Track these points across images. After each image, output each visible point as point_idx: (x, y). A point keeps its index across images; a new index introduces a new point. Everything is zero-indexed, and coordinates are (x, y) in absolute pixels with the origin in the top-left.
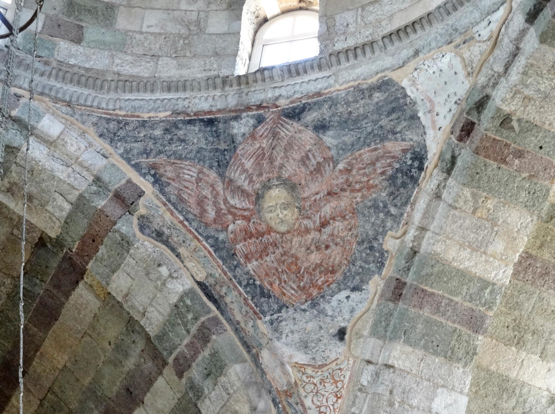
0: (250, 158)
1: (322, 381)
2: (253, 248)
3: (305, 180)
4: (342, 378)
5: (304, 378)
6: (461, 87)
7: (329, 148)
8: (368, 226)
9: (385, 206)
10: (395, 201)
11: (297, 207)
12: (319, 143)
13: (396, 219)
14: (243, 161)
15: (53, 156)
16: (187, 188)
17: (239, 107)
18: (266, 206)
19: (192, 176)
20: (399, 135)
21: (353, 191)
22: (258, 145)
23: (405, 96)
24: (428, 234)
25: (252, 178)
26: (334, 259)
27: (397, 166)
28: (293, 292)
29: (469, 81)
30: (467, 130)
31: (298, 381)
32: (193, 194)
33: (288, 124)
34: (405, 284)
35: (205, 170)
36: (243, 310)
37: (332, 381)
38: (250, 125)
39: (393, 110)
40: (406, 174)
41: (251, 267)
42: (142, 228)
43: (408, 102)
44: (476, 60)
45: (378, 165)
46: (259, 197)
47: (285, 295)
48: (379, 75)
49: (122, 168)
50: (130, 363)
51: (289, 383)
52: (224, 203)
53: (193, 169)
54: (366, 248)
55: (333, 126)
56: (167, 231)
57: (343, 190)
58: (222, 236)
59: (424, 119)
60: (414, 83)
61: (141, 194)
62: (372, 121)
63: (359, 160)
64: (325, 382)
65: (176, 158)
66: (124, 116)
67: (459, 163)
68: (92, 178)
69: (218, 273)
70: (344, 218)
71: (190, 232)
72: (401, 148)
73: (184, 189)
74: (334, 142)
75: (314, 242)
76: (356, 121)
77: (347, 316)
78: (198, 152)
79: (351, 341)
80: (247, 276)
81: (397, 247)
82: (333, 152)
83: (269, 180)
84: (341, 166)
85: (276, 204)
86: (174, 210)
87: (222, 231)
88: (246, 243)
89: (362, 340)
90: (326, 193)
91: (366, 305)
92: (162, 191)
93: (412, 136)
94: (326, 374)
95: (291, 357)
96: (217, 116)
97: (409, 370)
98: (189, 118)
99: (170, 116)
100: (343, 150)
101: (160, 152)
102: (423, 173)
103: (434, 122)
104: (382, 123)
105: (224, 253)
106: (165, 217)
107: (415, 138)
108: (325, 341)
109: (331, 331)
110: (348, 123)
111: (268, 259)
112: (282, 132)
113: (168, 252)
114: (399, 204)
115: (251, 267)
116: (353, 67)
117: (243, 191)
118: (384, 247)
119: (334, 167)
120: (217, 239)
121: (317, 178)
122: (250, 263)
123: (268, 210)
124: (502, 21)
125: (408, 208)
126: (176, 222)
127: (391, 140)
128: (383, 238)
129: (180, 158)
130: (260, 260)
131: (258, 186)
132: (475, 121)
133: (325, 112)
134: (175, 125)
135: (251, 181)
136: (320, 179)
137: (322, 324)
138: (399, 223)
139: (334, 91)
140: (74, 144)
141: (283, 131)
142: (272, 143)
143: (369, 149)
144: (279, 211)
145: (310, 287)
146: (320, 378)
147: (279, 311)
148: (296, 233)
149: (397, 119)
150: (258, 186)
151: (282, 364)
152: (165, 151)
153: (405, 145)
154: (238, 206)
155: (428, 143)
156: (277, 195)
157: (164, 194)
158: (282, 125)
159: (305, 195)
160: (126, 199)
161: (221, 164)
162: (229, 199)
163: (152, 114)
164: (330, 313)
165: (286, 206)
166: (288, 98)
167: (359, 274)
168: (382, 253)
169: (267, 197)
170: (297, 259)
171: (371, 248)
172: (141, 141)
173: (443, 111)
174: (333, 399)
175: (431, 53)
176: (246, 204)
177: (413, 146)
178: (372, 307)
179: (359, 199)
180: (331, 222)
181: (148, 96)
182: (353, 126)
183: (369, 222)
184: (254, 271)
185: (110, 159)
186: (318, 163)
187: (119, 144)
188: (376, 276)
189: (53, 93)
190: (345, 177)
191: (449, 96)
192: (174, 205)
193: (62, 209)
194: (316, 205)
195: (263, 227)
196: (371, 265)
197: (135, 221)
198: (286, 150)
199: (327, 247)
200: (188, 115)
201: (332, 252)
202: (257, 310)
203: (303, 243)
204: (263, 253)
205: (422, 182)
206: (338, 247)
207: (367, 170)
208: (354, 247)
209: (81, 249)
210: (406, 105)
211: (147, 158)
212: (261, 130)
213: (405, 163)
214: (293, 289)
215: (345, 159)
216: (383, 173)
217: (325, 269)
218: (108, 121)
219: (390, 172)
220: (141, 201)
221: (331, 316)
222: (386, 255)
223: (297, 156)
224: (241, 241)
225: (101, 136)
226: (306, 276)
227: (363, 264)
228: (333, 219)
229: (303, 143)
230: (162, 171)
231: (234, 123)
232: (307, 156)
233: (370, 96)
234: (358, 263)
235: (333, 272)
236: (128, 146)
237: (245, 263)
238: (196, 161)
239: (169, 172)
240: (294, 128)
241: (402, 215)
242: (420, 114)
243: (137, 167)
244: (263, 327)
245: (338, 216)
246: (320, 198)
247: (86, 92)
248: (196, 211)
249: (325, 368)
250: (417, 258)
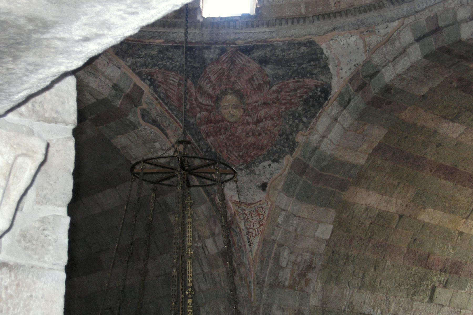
1: (251, 213)
3: (250, 93)
4: (263, 213)
5: (240, 210)
7: (268, 76)
8: (287, 126)
9: (300, 116)
10: (306, 114)
11: (243, 109)
13: (306, 125)
14: (210, 75)
15: (88, 71)
16: (172, 89)
17: (210, 42)
18: (222, 105)
20: (314, 76)
21: (281, 104)
22: (221, 67)
23: (322, 53)
24: (326, 140)
25: (215, 87)
27: (311, 94)
28: (235, 158)
29: (366, 55)
31: (235, 212)
32: (175, 93)
33: (242, 56)
34: (308, 165)
37: (257, 214)
38: (217, 53)
39: (312, 60)
40: (316, 99)
41: (209, 141)
42: (143, 117)
43: (323, 58)
44: (374, 44)
45: (299, 91)
46: (218, 99)
47: (229, 159)
48: (307, 37)
49: (130, 75)
52: (195, 101)
53: (176, 77)
54: (284, 138)
55: (271, 62)
57: (273, 102)
58: (192, 121)
60: (329, 47)
61: (142, 92)
62: (298, 63)
63: (286, 86)
64: (252, 214)
65: (165, 70)
66: (133, 41)
67: (352, 103)
68: (112, 84)
70: (272, 119)
71: (172, 117)
72: (314, 84)
74: (272, 72)
77: (268, 176)
78: (180, 67)
79: (269, 191)
80: (207, 146)
81: (304, 141)
82: (270, 79)
83: (226, 90)
84: (274, 88)
85: (229, 105)
86: (163, 103)
87: (192, 117)
88: (208, 126)
89: (276, 192)
90: (262, 102)
91: (280, 171)
92: (155, 90)
93: (323, 78)
94: (253, 209)
95: (231, 197)
96: (195, 45)
97: (307, 217)
98: (176, 45)
99: (163, 43)
100: (277, 78)
101: (155, 65)
102: (327, 102)
103: (338, 73)
104: (304, 66)
107: (325, 80)
109: (257, 184)
111: (221, 137)
114: (309, 116)
118: (296, 139)
119: (270, 88)
121: (258, 93)
122: (209, 138)
124: (396, 29)
125: (314, 120)
126: (163, 111)
127: (308, 78)
128: (296, 135)
129: (168, 69)
130: (215, 137)
131: (218, 92)
132: (368, 82)
133: (267, 53)
134: (166, 49)
136: (259, 94)
137: (251, 178)
138: (307, 127)
139: (275, 41)
142: (230, 67)
145: (246, 156)
146: (249, 211)
148: (240, 124)
149: (314, 66)
150: (218, 92)
154: (204, 103)
155: (333, 85)
156: (230, 99)
158: (238, 56)
159: (249, 102)
160: (134, 98)
162: (198, 98)
163: (151, 40)
164: (257, 173)
165: (235, 107)
166: (244, 40)
167: (278, 152)
170: (240, 139)
171: (288, 139)
172: (143, 58)
174: (257, 225)
175: (344, 32)
177: (322, 84)
178: (284, 173)
179: (283, 109)
180: (264, 120)
183: (288, 124)
185: (122, 69)
186: (260, 84)
187: (128, 59)
188: (289, 155)
191: (351, 60)
192: (162, 99)
194: (256, 109)
195: (219, 118)
196: (287, 149)
197: (139, 112)
198: (239, 73)
199: (260, 135)
200: (176, 43)
204: (218, 133)
205: (325, 106)
206: (267, 135)
207: (291, 93)
210: (322, 58)
211: (146, 68)
212: (224, 57)
213: (316, 93)
214: (235, 156)
216: (301, 97)
219: (305, 97)
220: (143, 99)
221: (258, 175)
222: (297, 144)
223: (246, 78)
224: (204, 124)
225: (116, 54)
226: (244, 149)
227: (281, 147)
228: (266, 119)
231: (206, 51)
232: (253, 79)
233: (299, 48)
234: (278, 146)
235: (262, 149)
236: (134, 61)
237: (206, 138)
238: (179, 72)
239: (160, 78)
240: (246, 59)
241: (310, 123)
242: (330, 66)
243: (139, 74)
245: (269, 118)
248: (177, 104)
249: (253, 206)
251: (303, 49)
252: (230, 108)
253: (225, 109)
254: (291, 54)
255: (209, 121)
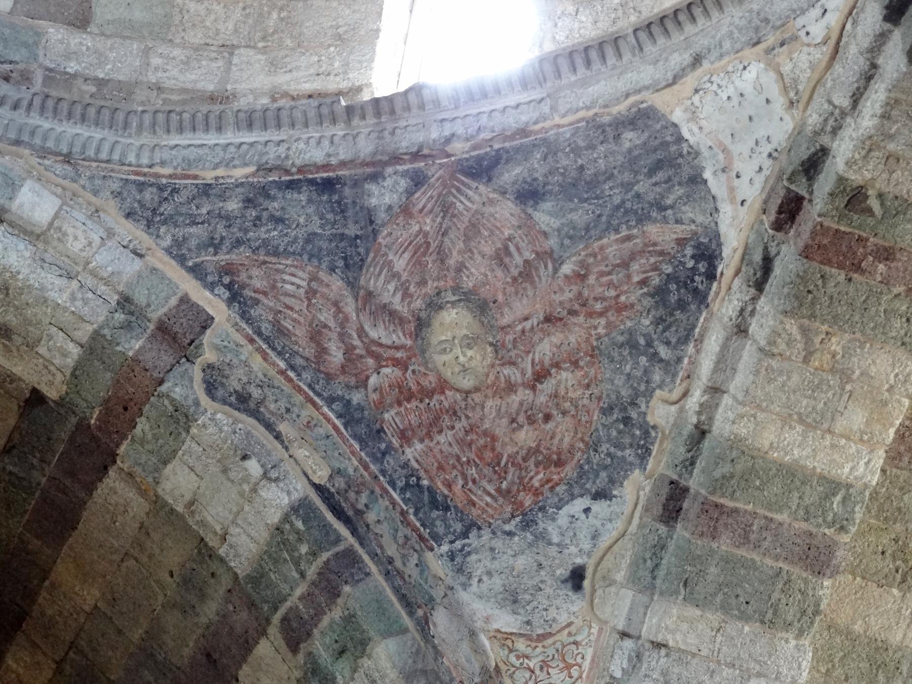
0: (404, 252)
2: (413, 419)
3: (505, 294)
4: (579, 660)
5: (512, 659)
6: (779, 127)
7: (545, 234)
8: (619, 381)
9: (649, 344)
10: (667, 334)
11: (491, 344)
12: (527, 223)
13: (670, 367)
14: (391, 257)
15: (43, 260)
16: (291, 309)
17: (379, 157)
18: (434, 340)
19: (299, 287)
20: (669, 212)
21: (590, 315)
22: (417, 228)
23: (680, 139)
24: (726, 400)
25: (408, 289)
26: (562, 440)
27: (669, 270)
28: (488, 499)
29: (793, 117)
30: (789, 210)
31: (501, 665)
32: (302, 320)
33: (470, 188)
34: (686, 490)
35: (321, 274)
36: (400, 534)
37: (562, 665)
38: (401, 190)
40: (685, 284)
41: (413, 452)
42: (210, 388)
43: (685, 152)
44: (805, 77)
45: (635, 267)
46: (421, 325)
47: (474, 504)
48: (632, 99)
49: (170, 274)
50: (210, 610)
51: (484, 670)
52: (359, 337)
53: (300, 273)
54: (617, 420)
55: (551, 192)
56: (256, 393)
57: (572, 313)
58: (357, 397)
59: (715, 184)
60: (693, 114)
61: (206, 322)
62: (622, 185)
63: (599, 257)
64: (548, 666)
65: (268, 254)
66: (170, 176)
67: (777, 270)
68: (116, 297)
69: (351, 465)
70: (575, 364)
71: (300, 390)
72: (675, 236)
73: (286, 310)
75: (524, 408)
76: (593, 184)
77: (586, 546)
78: (308, 241)
79: (594, 591)
80: (405, 471)
81: (672, 420)
83: (438, 294)
84: (567, 269)
85: (454, 338)
86: (269, 351)
87: (357, 387)
88: (402, 409)
89: (613, 589)
90: (542, 318)
91: (619, 525)
92: (244, 315)
93: (694, 215)
94: (551, 651)
95: (487, 620)
96: (340, 173)
97: (695, 650)
98: (288, 178)
99: (253, 175)
100: (571, 238)
101: (238, 243)
102: (715, 284)
103: (732, 190)
104: (639, 188)
105: (362, 430)
106: (254, 365)
107: (700, 219)
108: (548, 590)
109: (558, 572)
110: (580, 186)
111: (442, 438)
112: (458, 204)
113: (259, 431)
114: (674, 340)
115: (413, 452)
116: (584, 83)
117: (393, 314)
118: (649, 418)
119: (556, 270)
120: (349, 402)
121: (525, 289)
122: (409, 447)
123: (439, 348)
124: (846, 11)
125: (691, 349)
126: (272, 372)
127: (655, 221)
128: (648, 402)
129: (276, 254)
130: (427, 441)
131: (418, 304)
132: (803, 193)
133: (535, 167)
134: (264, 191)
135: (406, 295)
136: (530, 293)
137: (541, 558)
138: (674, 375)
139: (551, 129)
140: (79, 236)
141: (461, 202)
142: (441, 224)
143: (618, 236)
144: (458, 351)
145: (519, 491)
146: (541, 658)
147: (465, 535)
148: (490, 392)
149: (666, 182)
150: (418, 304)
151: (473, 634)
152: (248, 240)
153: (682, 230)
155: (723, 229)
157: (249, 320)
158: (458, 190)
159: (505, 321)
160: (180, 334)
161: (351, 262)
162: (367, 328)
163: (220, 172)
164: (556, 540)
165: (470, 342)
166: (467, 140)
167: (606, 467)
168: (647, 430)
169: (436, 324)
170: (494, 439)
171: (626, 420)
172: (202, 223)
173: (747, 168)
175: (723, 62)
176: (399, 338)
177: (696, 233)
178: (630, 529)
179: (601, 331)
180: (553, 371)
181: (212, 139)
182: (587, 192)
183: (622, 373)
184: (417, 461)
185: (147, 258)
186: (527, 262)
187: (163, 229)
188: (637, 471)
189: (38, 141)
190: (575, 288)
191: (757, 143)
192: (267, 340)
193: (65, 355)
195: (430, 381)
196: (628, 451)
198: (467, 239)
199: (548, 418)
200: (287, 172)
201: (556, 427)
202: (426, 533)
203: (503, 410)
204: (433, 426)
205: (714, 300)
206: (568, 419)
207: (614, 277)
208: (595, 418)
209: (104, 419)
210: (681, 155)
211: (216, 254)
212: (421, 198)
213: (683, 264)
214: (489, 494)
215: (575, 254)
216: (643, 283)
217: (545, 457)
218: (141, 186)
219: (656, 281)
220: (207, 338)
221: (558, 545)
222: (653, 434)
223: (488, 249)
224: (391, 406)
225: (128, 215)
226: (511, 470)
227: (612, 450)
228: (557, 365)
229: (498, 225)
230: (243, 277)
232: (506, 248)
233: (617, 137)
234: (604, 448)
235: (559, 463)
236: (180, 233)
237: (402, 446)
238: (306, 257)
239: (257, 279)
240: (481, 195)
241: (679, 360)
242: (707, 175)
243: (197, 271)
244: (437, 564)
245: (565, 362)
246: (532, 328)
247: (98, 134)
249: (550, 641)
250: (706, 444)
251: (630, 138)
252: (456, 348)
253: (444, 351)
254: (601, 158)
255: (405, 395)
